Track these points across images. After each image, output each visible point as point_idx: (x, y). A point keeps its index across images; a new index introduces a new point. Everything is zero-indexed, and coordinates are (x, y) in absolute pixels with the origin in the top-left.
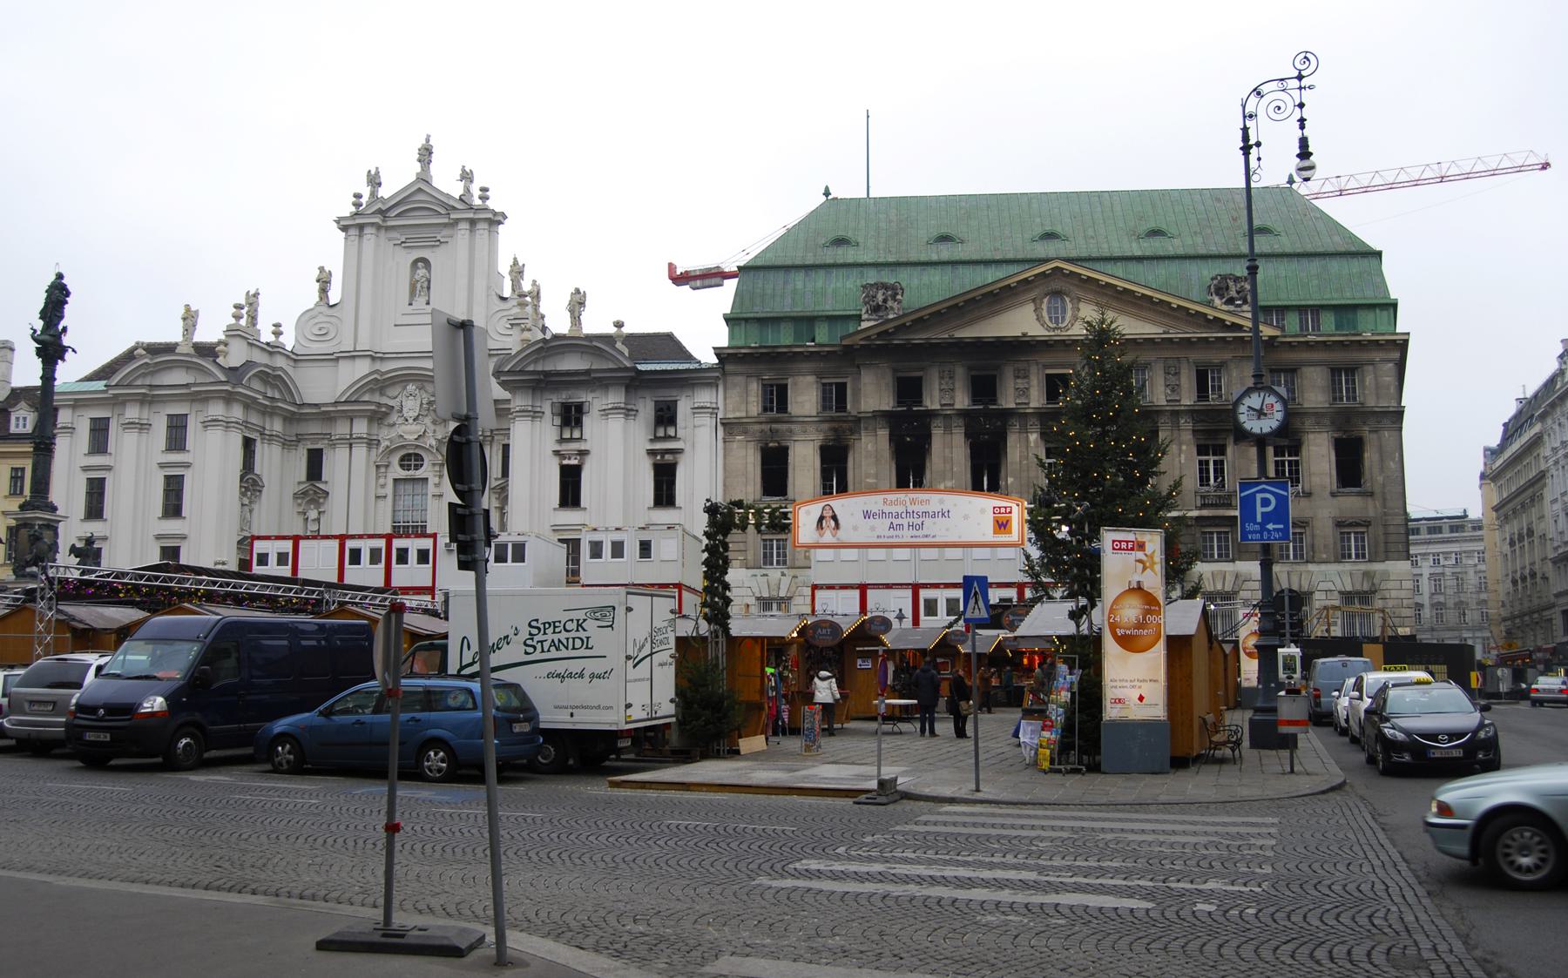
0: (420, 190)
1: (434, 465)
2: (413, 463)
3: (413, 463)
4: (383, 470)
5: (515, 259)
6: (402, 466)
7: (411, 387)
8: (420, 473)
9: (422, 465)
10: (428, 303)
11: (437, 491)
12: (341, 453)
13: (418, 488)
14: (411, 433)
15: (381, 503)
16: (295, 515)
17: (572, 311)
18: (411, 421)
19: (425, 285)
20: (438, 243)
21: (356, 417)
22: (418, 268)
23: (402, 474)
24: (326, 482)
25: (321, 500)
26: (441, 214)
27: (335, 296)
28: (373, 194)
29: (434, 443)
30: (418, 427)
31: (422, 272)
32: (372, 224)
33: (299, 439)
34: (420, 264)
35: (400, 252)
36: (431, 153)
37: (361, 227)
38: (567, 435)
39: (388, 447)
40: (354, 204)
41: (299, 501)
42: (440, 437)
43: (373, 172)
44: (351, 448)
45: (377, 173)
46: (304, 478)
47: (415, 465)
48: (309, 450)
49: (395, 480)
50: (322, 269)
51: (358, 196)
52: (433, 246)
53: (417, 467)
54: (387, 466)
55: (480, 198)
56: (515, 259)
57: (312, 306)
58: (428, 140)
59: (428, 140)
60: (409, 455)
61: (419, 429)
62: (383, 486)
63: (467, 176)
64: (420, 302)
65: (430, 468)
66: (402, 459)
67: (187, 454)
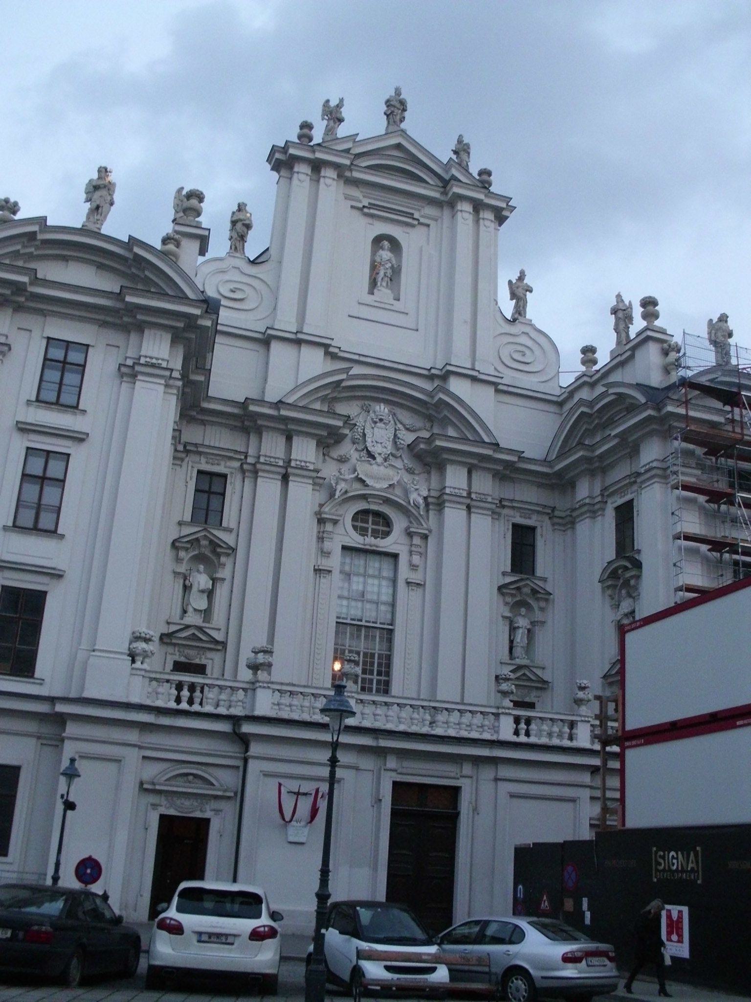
0: (399, 146)
1: (410, 535)
3: (370, 526)
4: (329, 527)
6: (355, 528)
7: (382, 409)
8: (387, 544)
9: (387, 534)
11: (416, 577)
13: (374, 564)
14: (378, 479)
15: (324, 581)
17: (714, 343)
18: (379, 459)
19: (389, 272)
20: (416, 222)
21: (299, 433)
22: (382, 248)
23: (356, 540)
24: (230, 530)
25: (223, 559)
26: (427, 183)
27: (252, 250)
28: (329, 131)
29: (421, 501)
30: (390, 472)
31: (385, 254)
32: (336, 166)
34: (386, 244)
35: (361, 221)
36: (404, 110)
37: (317, 166)
39: (346, 492)
41: (182, 554)
42: (425, 493)
45: (339, 106)
46: (188, 517)
47: (374, 531)
48: (200, 472)
49: (345, 548)
51: (306, 126)
52: (407, 224)
53: (376, 534)
54: (335, 522)
60: (366, 512)
62: (326, 554)
63: (462, 150)
64: (384, 293)
65: (404, 540)
66: (354, 519)
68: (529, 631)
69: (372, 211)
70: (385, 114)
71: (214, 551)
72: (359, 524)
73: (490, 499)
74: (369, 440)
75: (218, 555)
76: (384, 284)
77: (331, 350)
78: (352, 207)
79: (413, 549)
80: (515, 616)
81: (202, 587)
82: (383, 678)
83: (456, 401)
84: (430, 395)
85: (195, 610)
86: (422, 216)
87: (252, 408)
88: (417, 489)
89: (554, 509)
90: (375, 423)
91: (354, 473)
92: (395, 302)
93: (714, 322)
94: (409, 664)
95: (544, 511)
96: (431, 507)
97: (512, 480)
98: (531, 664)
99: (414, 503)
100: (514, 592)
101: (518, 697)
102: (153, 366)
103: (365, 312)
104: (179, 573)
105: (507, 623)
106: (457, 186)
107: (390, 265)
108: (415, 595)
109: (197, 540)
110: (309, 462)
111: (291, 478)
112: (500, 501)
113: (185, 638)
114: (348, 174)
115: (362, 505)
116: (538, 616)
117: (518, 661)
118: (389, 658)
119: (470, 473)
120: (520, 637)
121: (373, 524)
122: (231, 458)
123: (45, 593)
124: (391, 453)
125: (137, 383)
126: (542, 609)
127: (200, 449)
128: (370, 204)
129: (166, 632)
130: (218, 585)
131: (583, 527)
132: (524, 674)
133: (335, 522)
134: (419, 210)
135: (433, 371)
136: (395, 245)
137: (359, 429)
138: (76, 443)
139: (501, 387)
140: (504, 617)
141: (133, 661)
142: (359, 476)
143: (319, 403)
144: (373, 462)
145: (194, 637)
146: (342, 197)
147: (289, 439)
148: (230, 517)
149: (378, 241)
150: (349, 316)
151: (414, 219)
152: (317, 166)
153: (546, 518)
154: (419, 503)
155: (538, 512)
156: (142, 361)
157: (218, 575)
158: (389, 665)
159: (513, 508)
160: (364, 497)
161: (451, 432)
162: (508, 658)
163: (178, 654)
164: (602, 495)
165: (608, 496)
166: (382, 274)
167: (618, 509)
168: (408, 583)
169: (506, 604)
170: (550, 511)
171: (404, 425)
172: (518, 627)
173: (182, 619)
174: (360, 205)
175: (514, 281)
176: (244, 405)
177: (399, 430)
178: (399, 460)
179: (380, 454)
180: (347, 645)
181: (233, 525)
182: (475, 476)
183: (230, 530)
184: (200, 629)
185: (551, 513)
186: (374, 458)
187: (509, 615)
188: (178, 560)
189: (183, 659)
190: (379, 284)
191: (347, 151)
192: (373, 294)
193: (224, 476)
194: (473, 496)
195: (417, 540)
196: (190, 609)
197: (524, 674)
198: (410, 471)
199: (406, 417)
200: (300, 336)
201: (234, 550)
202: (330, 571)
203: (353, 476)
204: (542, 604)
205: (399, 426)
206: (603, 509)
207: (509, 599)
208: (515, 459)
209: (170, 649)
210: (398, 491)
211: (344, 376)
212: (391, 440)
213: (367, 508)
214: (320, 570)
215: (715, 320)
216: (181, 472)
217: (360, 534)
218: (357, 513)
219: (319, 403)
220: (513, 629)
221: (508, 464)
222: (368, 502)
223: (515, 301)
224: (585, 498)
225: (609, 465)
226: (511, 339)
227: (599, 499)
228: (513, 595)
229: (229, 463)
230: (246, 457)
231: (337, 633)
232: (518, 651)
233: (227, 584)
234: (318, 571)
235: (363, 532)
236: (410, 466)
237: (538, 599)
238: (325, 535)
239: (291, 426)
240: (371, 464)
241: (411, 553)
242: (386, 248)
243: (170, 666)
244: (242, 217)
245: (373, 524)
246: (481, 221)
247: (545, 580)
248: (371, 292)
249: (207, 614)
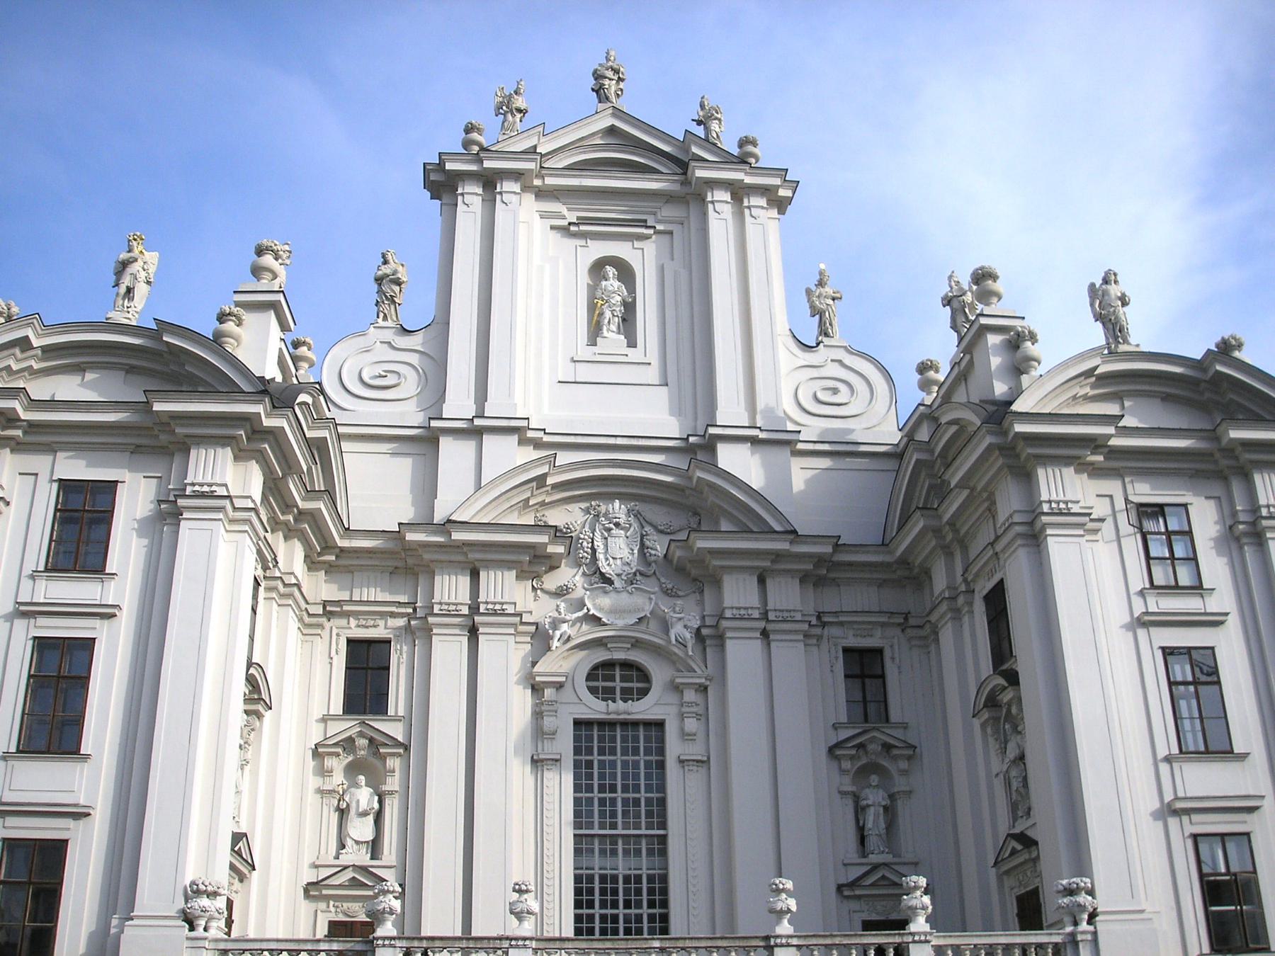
0: (612, 131)
1: (677, 689)
2: (618, 684)
3: (618, 684)
6: (593, 691)
7: (618, 509)
8: (642, 709)
9: (644, 692)
10: (632, 344)
11: (695, 750)
15: (551, 777)
16: (312, 799)
20: (651, 231)
23: (596, 708)
31: (612, 283)
32: (516, 175)
33: (330, 610)
34: (611, 271)
37: (489, 181)
38: (1159, 579)
39: (569, 639)
41: (329, 762)
46: (337, 707)
47: (624, 691)
48: (350, 642)
49: (577, 723)
53: (627, 695)
60: (608, 665)
61: (641, 603)
67: (112, 585)
68: (886, 808)
69: (583, 228)
70: (593, 90)
71: (376, 754)
72: (601, 684)
73: (798, 617)
74: (601, 557)
75: (383, 758)
76: (614, 328)
77: (530, 434)
78: (552, 228)
79: (685, 709)
80: (863, 788)
81: (363, 806)
82: (656, 911)
83: (724, 478)
84: (685, 474)
85: (357, 842)
86: (659, 222)
87: (410, 537)
88: (680, 619)
89: (906, 616)
90: (609, 530)
91: (582, 609)
92: (630, 351)
93: (1097, 286)
94: (694, 886)
95: (892, 621)
96: (708, 642)
97: (835, 583)
98: (896, 860)
99: (676, 640)
100: (853, 752)
101: (877, 914)
102: (203, 495)
103: (585, 372)
104: (331, 792)
105: (850, 802)
107: (619, 298)
108: (695, 779)
109: (350, 740)
110: (506, 603)
111: (481, 630)
112: (819, 617)
113: (340, 886)
114: (537, 182)
115: (601, 656)
116: (900, 784)
117: (874, 858)
118: (664, 879)
119: (762, 581)
120: (874, 821)
121: (622, 681)
122: (393, 615)
123: (67, 841)
124: (637, 570)
125: (182, 523)
126: (904, 773)
127: (345, 608)
128: (578, 218)
129: (315, 881)
130: (387, 802)
131: (947, 635)
132: (883, 877)
134: (655, 214)
135: (692, 439)
136: (626, 273)
137: (585, 544)
138: (106, 622)
139: (800, 446)
140: (843, 794)
141: (192, 928)
142: (591, 613)
143: (516, 513)
144: (609, 588)
145: (355, 883)
146: (537, 216)
147: (475, 575)
148: (397, 698)
149: (598, 268)
150: (559, 382)
151: (647, 227)
152: (489, 181)
153: (898, 631)
154: (685, 640)
155: (883, 625)
156: (189, 490)
158: (664, 891)
159: (841, 624)
160: (599, 643)
161: (725, 526)
162: (856, 855)
163: (332, 909)
164: (965, 580)
165: (973, 581)
166: (608, 314)
167: (987, 598)
168: (681, 762)
169: (843, 772)
170: (902, 621)
171: (655, 527)
172: (868, 806)
173: (337, 858)
174: (565, 223)
175: (814, 288)
176: (397, 536)
177: (647, 535)
178: (653, 579)
179: (618, 575)
180: (597, 867)
182: (770, 583)
183: (396, 719)
184: (364, 869)
185: (904, 622)
186: (610, 582)
187: (850, 788)
188: (323, 772)
189: (341, 918)
190: (605, 328)
191: (533, 150)
192: (595, 344)
193: (388, 642)
194: (771, 616)
195: (690, 695)
196: (349, 842)
197: (883, 877)
198: (668, 593)
199: (658, 515)
200: (477, 422)
201: (407, 748)
202: (557, 760)
203: (580, 614)
204: (903, 765)
205: (648, 529)
206: (970, 604)
207: (846, 765)
208: (829, 549)
209: (322, 905)
210: (653, 626)
211: (545, 469)
212: (636, 551)
213: (610, 657)
214: (542, 761)
215: (1098, 283)
216: (320, 645)
217: (603, 699)
218: (595, 668)
219: (516, 513)
220: (859, 810)
221: (820, 560)
222: (609, 649)
223: (817, 316)
224: (943, 591)
225: (967, 532)
226: (815, 373)
227: (963, 588)
228: (852, 758)
229: (392, 622)
230: (415, 610)
231: (578, 852)
232: (872, 842)
235: (608, 695)
236: (670, 586)
237: (895, 758)
238: (544, 708)
239: (473, 556)
240: (606, 592)
241: (682, 717)
242: (611, 275)
243: (322, 931)
244: (388, 271)
245: (622, 681)
246: (747, 212)
247: (905, 726)
248: (592, 342)
249: (375, 847)
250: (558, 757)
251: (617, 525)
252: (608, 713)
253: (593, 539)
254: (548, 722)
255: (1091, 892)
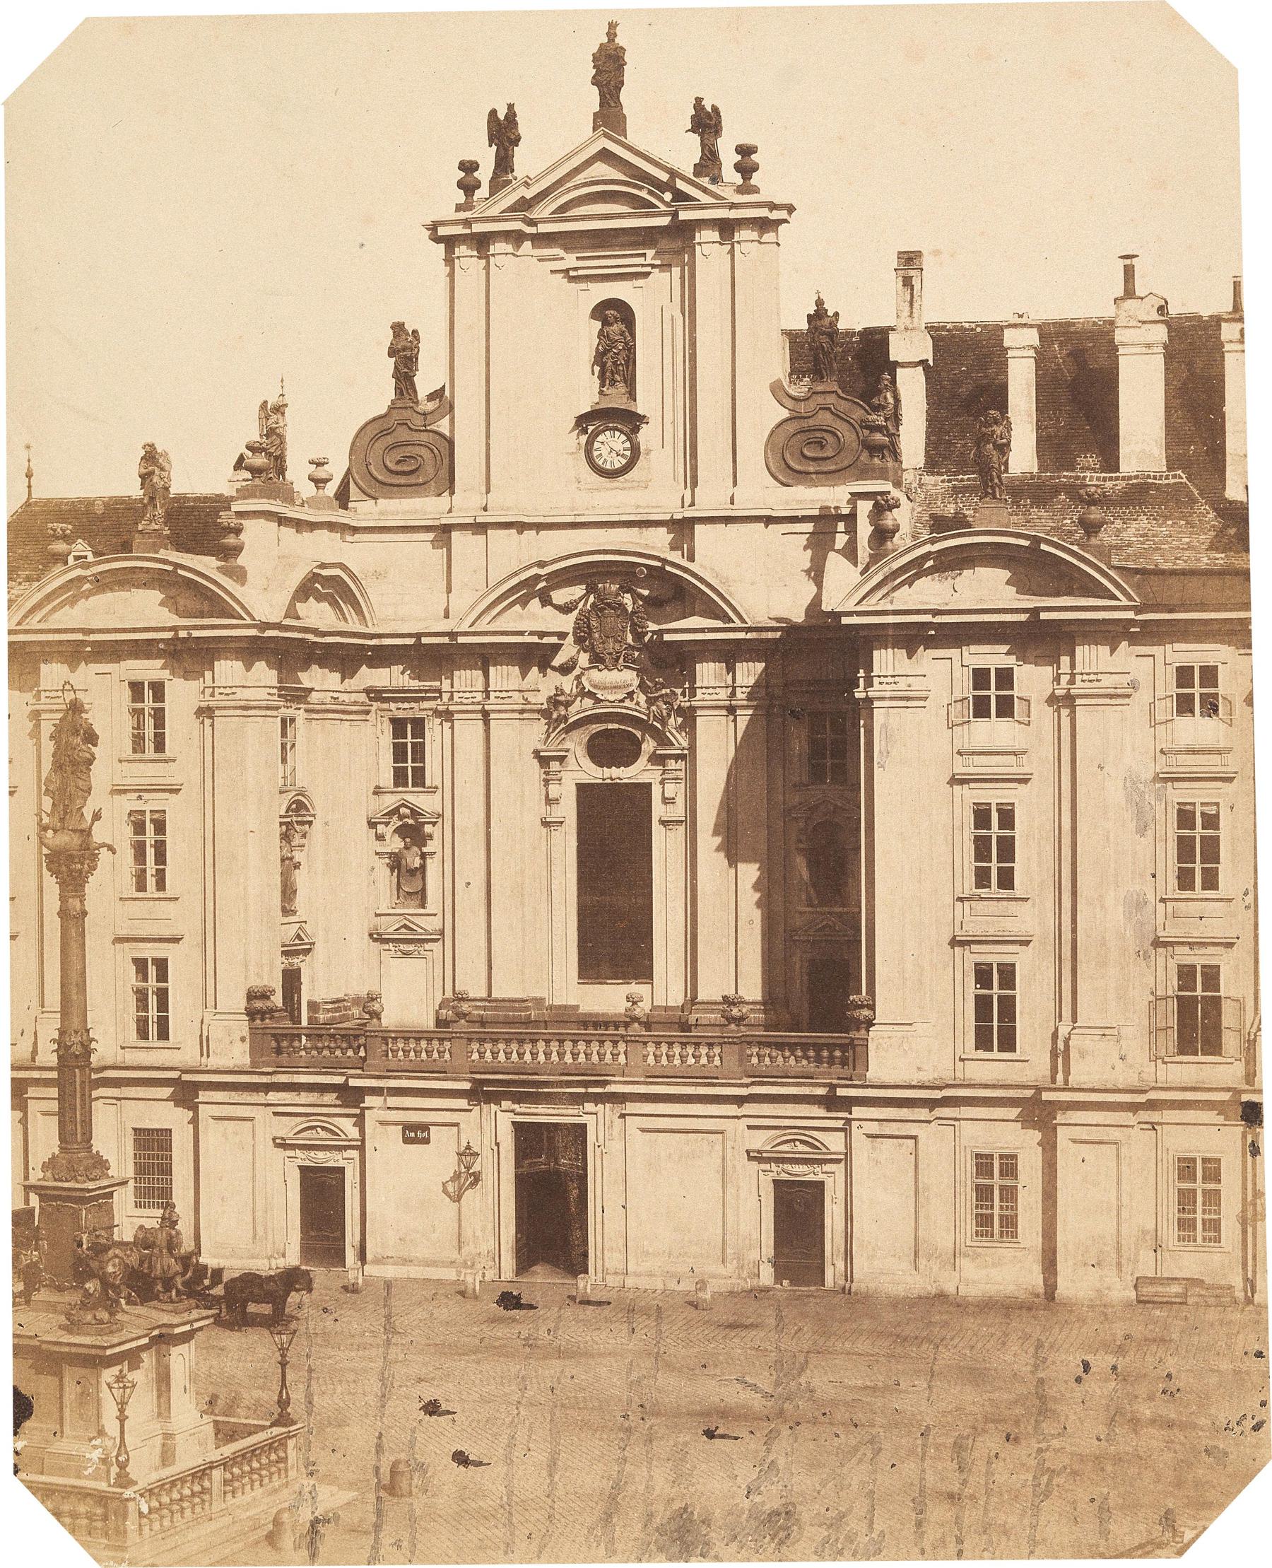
4: (555, 766)
5: (819, 303)
12: (469, 732)
15: (558, 834)
20: (648, 269)
23: (595, 774)
32: (506, 235)
37: (482, 242)
40: (460, 185)
43: (501, 116)
44: (487, 723)
46: (387, 779)
50: (398, 328)
51: (469, 167)
54: (561, 759)
55: (738, 167)
56: (819, 303)
57: (383, 411)
58: (611, 35)
59: (611, 35)
90: (602, 610)
106: (686, 209)
130: (429, 861)
133: (561, 759)
157: (425, 850)
163: (393, 949)
179: (610, 654)
181: (438, 782)
188: (380, 838)
202: (562, 822)
233: (438, 857)
234: (545, 824)
250: (562, 820)
251: (609, 605)
252: (604, 780)
253: (588, 619)
254: (554, 790)
255: (872, 1007)
